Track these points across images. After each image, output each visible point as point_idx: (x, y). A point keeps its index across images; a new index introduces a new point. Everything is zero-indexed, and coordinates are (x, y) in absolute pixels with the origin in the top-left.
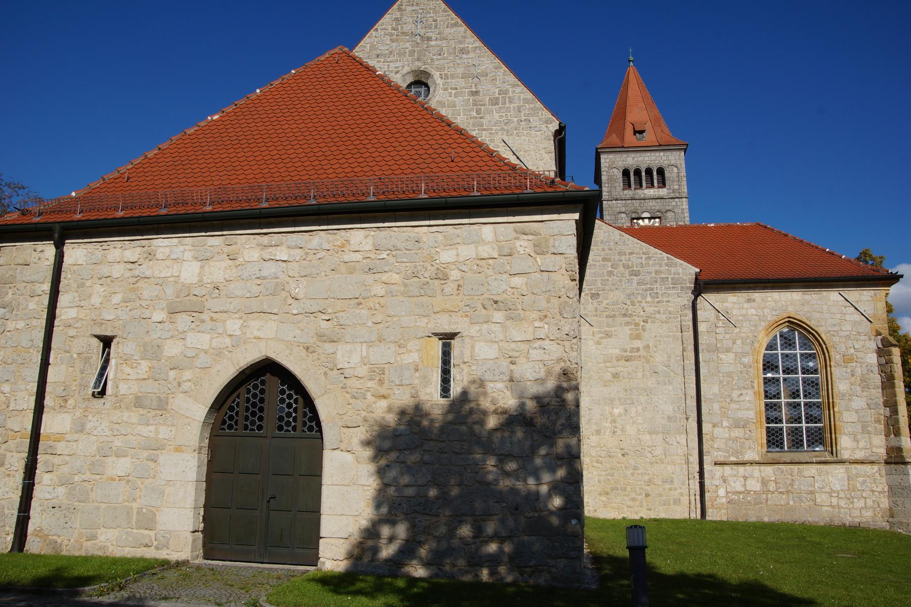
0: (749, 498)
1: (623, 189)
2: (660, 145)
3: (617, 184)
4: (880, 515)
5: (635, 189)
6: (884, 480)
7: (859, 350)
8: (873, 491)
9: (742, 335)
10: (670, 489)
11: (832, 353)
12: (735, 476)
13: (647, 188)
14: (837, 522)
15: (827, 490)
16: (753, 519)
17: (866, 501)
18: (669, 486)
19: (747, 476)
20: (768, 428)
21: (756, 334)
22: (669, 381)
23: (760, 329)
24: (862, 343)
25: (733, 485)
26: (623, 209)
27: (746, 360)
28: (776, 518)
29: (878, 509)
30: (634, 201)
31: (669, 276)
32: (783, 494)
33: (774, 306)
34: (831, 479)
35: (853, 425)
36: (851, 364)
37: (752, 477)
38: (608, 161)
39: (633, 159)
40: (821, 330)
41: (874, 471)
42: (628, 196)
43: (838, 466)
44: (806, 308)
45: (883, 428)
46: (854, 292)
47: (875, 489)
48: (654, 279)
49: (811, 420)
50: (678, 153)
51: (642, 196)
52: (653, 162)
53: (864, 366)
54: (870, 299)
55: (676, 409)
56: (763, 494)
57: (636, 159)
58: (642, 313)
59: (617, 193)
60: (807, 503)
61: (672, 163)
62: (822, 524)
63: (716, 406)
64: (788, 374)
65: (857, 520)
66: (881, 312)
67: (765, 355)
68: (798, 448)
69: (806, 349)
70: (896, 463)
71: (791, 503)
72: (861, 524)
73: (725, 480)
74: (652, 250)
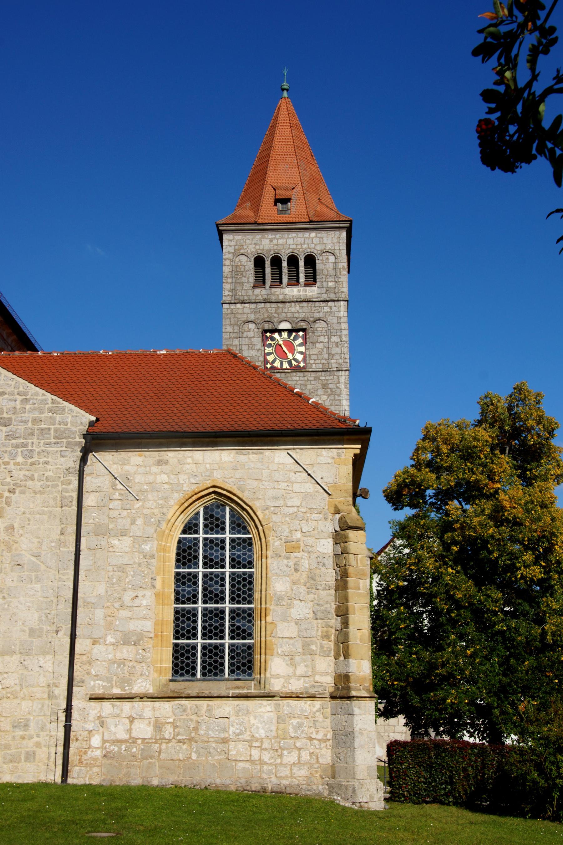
0: (134, 750)
1: (254, 287)
2: (311, 221)
3: (244, 280)
4: (318, 775)
5: (271, 286)
6: (328, 722)
7: (308, 534)
8: (311, 739)
9: (146, 511)
10: (23, 738)
11: (270, 539)
12: (118, 716)
13: (289, 285)
14: (255, 786)
15: (247, 736)
16: (136, 781)
17: (300, 754)
18: (21, 733)
19: (135, 716)
20: (176, 645)
21: (165, 510)
22: (37, 577)
23: (172, 502)
24: (313, 524)
25: (113, 729)
26: (252, 317)
27: (147, 547)
28: (170, 779)
29: (316, 766)
30: (268, 305)
31: (52, 427)
32: (184, 743)
33: (195, 470)
34: (252, 721)
35: (291, 641)
36: (295, 554)
37: (141, 717)
38: (232, 243)
39: (271, 241)
40: (256, 505)
41: (315, 709)
42: (260, 297)
43: (265, 702)
44: (238, 474)
45: (333, 647)
46: (310, 451)
47: (314, 736)
48: (30, 431)
49: (238, 635)
50: (336, 233)
51: (281, 297)
52: (299, 247)
53: (313, 556)
54: (330, 461)
55: (44, 618)
56: (156, 743)
58: (8, 480)
59: (244, 293)
60: (216, 757)
61: (327, 249)
62: (233, 788)
63: (99, 614)
64: (211, 567)
65: (285, 782)
66: (345, 480)
67: (179, 542)
68: (216, 675)
69: (239, 532)
70: (341, 698)
71: (194, 756)
72: (288, 789)
73: (103, 722)
74: (32, 389)
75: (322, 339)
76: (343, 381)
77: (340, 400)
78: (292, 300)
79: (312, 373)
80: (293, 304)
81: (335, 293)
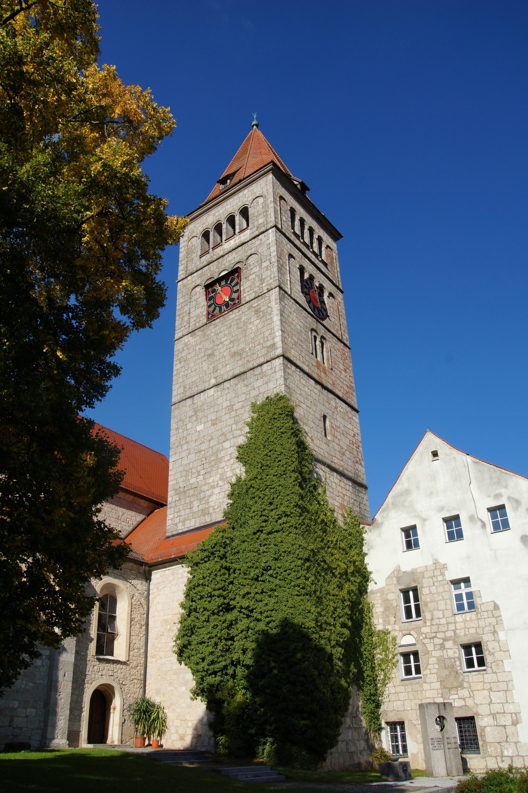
51: (221, 254)
57: (217, 214)
75: (254, 270)
76: (274, 298)
77: (271, 318)
78: (229, 250)
79: (247, 304)
80: (230, 254)
81: (264, 226)
